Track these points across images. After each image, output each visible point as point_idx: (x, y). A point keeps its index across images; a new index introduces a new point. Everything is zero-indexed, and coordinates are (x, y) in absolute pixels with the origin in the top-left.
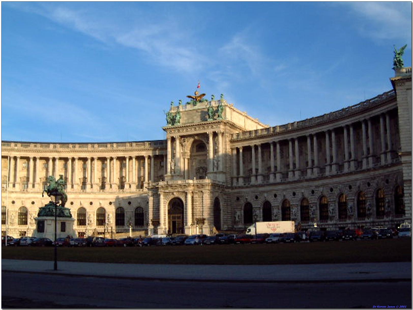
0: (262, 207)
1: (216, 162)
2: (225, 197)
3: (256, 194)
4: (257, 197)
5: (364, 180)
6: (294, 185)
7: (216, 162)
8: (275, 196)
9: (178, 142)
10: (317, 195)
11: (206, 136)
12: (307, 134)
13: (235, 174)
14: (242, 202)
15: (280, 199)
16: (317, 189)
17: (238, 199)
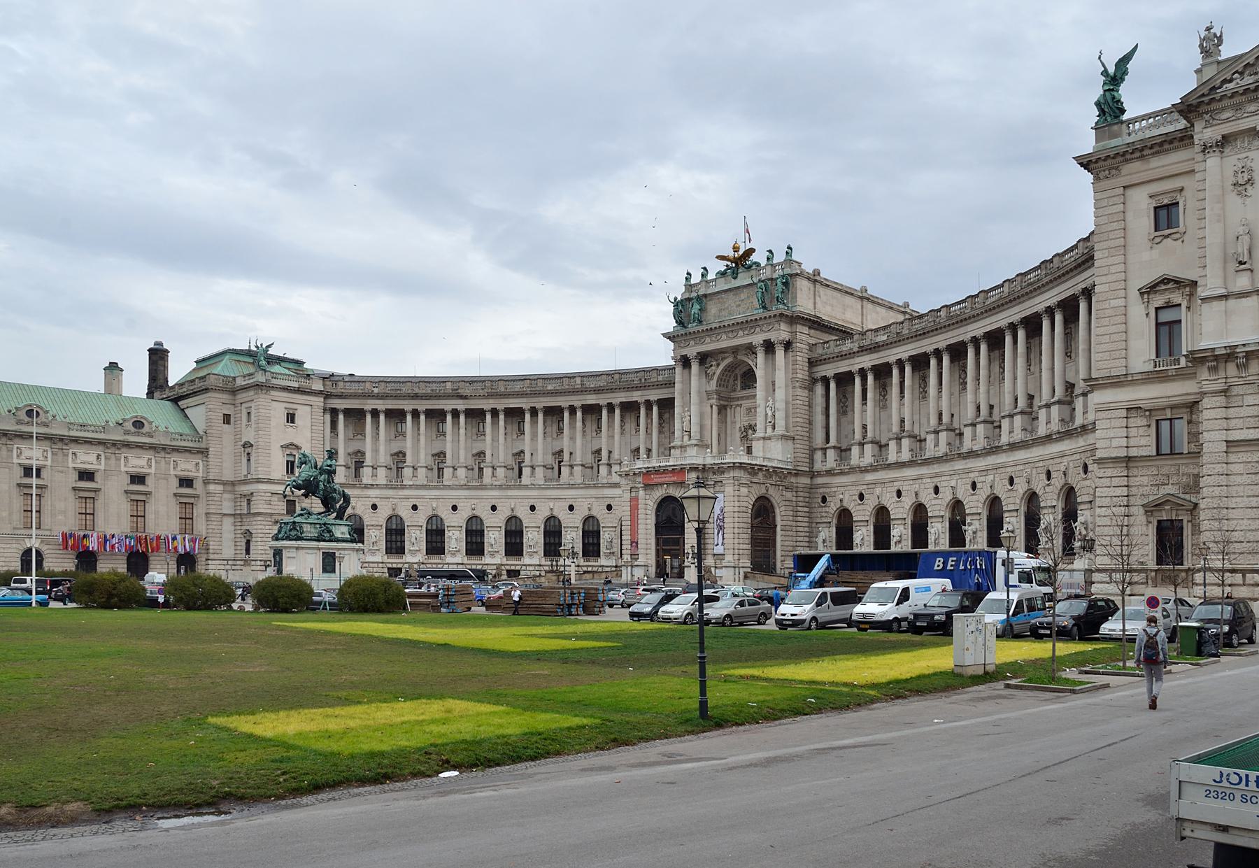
0: (835, 521)
1: (770, 413)
2: (789, 495)
3: (861, 488)
4: (861, 497)
5: (1078, 456)
6: (936, 469)
7: (770, 413)
8: (899, 494)
9: (695, 367)
10: (983, 493)
11: (751, 349)
12: (967, 337)
13: (819, 439)
14: (833, 507)
15: (908, 501)
16: (982, 479)
17: (824, 500)
